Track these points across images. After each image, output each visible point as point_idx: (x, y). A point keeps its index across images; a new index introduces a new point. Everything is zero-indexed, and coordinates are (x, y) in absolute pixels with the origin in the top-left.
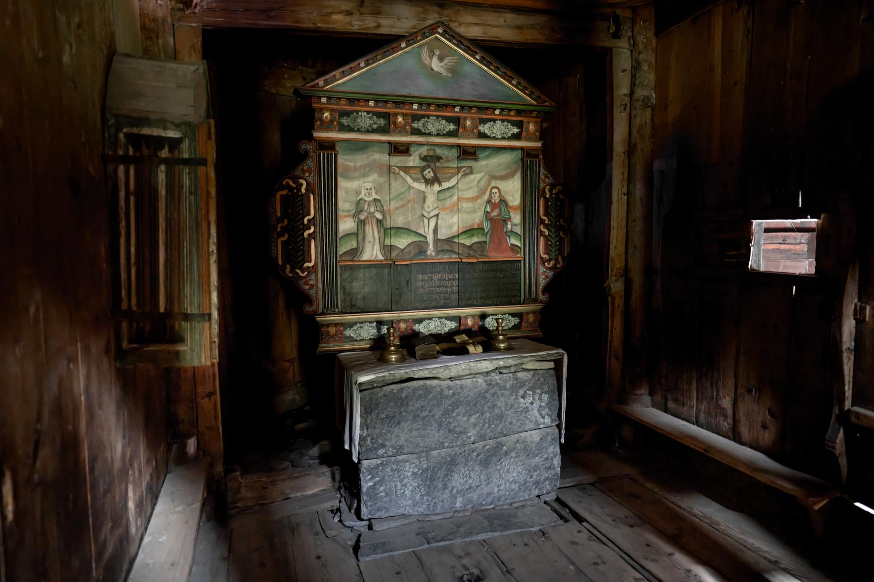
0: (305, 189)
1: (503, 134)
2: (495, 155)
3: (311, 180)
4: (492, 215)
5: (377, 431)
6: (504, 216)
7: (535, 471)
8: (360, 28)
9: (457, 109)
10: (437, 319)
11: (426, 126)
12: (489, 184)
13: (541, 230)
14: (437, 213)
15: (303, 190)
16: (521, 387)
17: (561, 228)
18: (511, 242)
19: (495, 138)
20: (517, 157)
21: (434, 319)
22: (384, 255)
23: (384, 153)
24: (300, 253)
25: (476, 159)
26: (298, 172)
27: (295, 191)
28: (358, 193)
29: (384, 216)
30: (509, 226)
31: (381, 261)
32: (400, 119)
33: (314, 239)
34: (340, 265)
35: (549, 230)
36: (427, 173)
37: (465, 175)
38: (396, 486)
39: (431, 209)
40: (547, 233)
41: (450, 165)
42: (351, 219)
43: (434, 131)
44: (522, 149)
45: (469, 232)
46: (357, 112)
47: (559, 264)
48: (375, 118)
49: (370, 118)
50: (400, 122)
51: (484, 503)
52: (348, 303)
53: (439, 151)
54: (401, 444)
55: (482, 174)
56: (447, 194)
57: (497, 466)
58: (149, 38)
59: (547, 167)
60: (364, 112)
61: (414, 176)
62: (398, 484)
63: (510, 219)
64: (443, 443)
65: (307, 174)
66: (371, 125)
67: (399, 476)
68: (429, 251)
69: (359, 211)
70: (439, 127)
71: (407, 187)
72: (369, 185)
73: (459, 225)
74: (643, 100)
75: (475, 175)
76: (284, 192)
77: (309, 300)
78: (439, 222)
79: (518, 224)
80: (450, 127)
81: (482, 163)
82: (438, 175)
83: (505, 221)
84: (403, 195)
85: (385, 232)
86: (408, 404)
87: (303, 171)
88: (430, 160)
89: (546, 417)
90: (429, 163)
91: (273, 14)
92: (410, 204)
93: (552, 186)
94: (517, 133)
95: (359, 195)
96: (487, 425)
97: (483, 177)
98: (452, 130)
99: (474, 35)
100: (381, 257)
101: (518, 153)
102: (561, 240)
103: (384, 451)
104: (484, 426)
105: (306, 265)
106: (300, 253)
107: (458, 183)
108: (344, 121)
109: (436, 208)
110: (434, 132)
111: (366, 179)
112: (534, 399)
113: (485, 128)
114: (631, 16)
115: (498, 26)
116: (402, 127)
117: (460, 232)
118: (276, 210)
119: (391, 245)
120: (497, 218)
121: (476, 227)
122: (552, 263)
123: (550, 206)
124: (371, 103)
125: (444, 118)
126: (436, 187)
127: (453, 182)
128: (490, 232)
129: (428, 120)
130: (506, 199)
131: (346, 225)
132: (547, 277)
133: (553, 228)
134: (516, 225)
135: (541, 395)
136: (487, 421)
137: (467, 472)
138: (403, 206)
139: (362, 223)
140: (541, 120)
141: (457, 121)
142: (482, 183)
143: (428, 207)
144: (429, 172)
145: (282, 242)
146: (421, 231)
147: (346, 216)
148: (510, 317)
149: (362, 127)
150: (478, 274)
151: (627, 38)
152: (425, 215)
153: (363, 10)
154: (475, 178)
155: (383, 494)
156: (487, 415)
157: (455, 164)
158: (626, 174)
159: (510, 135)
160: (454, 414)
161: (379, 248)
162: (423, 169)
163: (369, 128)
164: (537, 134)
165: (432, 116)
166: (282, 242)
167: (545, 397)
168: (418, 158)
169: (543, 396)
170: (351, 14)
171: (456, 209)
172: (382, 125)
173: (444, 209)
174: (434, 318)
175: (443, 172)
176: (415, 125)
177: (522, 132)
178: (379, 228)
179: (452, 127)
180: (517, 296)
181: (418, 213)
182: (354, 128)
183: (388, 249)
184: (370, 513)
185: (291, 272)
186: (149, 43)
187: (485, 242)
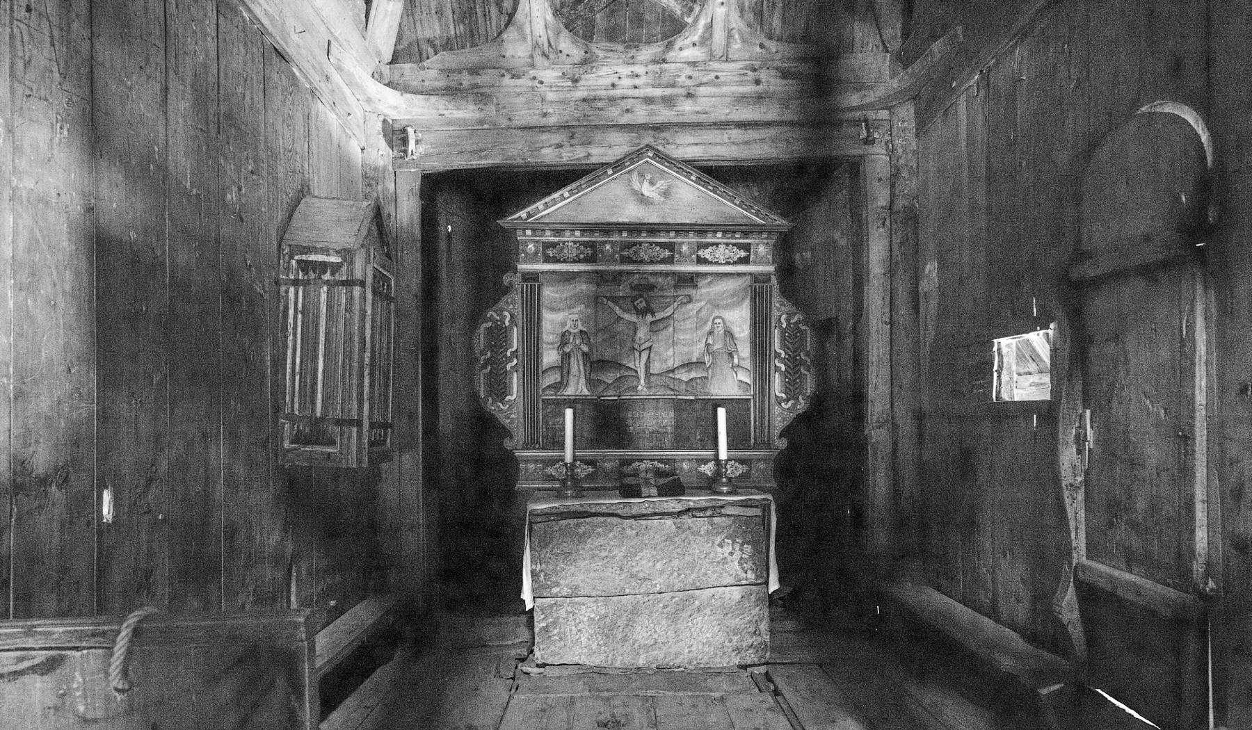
4: (715, 348)
5: (551, 567)
7: (735, 634)
14: (650, 344)
15: (507, 323)
16: (719, 533)
19: (717, 263)
24: (503, 386)
25: (695, 286)
26: (502, 304)
29: (591, 349)
30: (736, 361)
37: (683, 304)
38: (571, 630)
39: (643, 341)
42: (555, 352)
51: (672, 664)
53: (652, 280)
54: (576, 583)
57: (688, 622)
58: (369, 185)
62: (573, 628)
64: (623, 589)
65: (511, 307)
66: (577, 256)
67: (575, 620)
68: (640, 387)
72: (575, 317)
78: (652, 355)
81: (704, 291)
86: (586, 542)
87: (507, 303)
89: (749, 572)
91: (484, 153)
93: (790, 315)
96: (676, 574)
100: (587, 393)
103: (558, 590)
104: (672, 574)
105: (508, 398)
106: (503, 386)
112: (734, 549)
113: (706, 254)
117: (675, 366)
121: (694, 360)
126: (649, 318)
127: (669, 312)
132: (784, 419)
134: (743, 359)
135: (742, 545)
136: (676, 569)
137: (652, 625)
139: (566, 357)
144: (641, 302)
146: (631, 365)
148: (737, 464)
151: (883, 143)
153: (574, 142)
155: (556, 638)
156: (676, 563)
157: (672, 292)
158: (888, 299)
159: (735, 259)
160: (638, 558)
162: (634, 299)
167: (748, 548)
169: (745, 546)
170: (561, 146)
184: (542, 658)
186: (369, 189)
187: (706, 378)
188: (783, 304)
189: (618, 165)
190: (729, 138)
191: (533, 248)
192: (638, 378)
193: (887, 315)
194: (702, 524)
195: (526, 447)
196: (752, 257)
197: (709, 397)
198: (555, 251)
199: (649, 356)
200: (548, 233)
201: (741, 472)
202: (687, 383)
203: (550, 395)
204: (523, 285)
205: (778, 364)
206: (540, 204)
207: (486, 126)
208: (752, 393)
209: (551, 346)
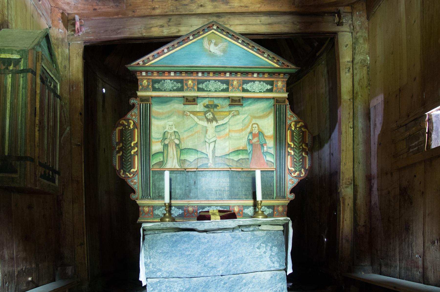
0: (133, 126)
1: (260, 89)
2: (254, 103)
3: (136, 121)
6: (262, 142)
8: (168, 33)
9: (228, 75)
10: (214, 207)
11: (208, 86)
12: (251, 121)
13: (288, 151)
14: (215, 140)
15: (132, 127)
17: (303, 150)
18: (267, 159)
19: (254, 92)
20: (271, 103)
21: (212, 207)
22: (180, 165)
23: (180, 103)
26: (129, 116)
27: (127, 127)
28: (164, 128)
30: (265, 149)
31: (178, 169)
32: (190, 82)
33: (137, 155)
34: (152, 171)
35: (294, 151)
36: (209, 115)
37: (234, 116)
39: (211, 137)
40: (293, 153)
41: (224, 110)
43: (213, 89)
44: (274, 98)
45: (237, 151)
46: (164, 80)
47: (302, 174)
48: (175, 83)
49: (172, 83)
50: (190, 84)
52: (157, 194)
53: (216, 102)
55: (246, 116)
56: (222, 128)
59: (292, 109)
60: (169, 80)
61: (200, 117)
63: (266, 144)
65: (134, 117)
66: (172, 87)
69: (164, 139)
70: (217, 87)
71: (195, 123)
72: (171, 123)
73: (230, 148)
74: (361, 62)
75: (241, 116)
76: (121, 128)
77: (133, 191)
78: (216, 145)
79: (272, 147)
80: (223, 86)
82: (216, 116)
83: (262, 146)
84: (192, 128)
85: (180, 152)
87: (132, 115)
88: (210, 107)
90: (209, 109)
92: (196, 134)
93: (296, 123)
94: (270, 89)
95: (165, 129)
97: (247, 117)
98: (224, 88)
99: (240, 31)
100: (178, 167)
101: (272, 102)
102: (303, 158)
105: (132, 170)
106: (129, 163)
107: (229, 121)
108: (156, 85)
109: (214, 137)
110: (213, 90)
111: (169, 120)
113: (247, 86)
114: (350, 11)
115: (255, 25)
116: (192, 87)
117: (230, 152)
118: (116, 138)
119: (185, 159)
120: (257, 143)
121: (241, 148)
122: (297, 173)
123: (295, 135)
124: (172, 74)
125: (219, 81)
126: (214, 124)
128: (251, 152)
129: (209, 83)
130: (263, 131)
131: (156, 147)
133: (297, 150)
134: (270, 148)
138: (192, 135)
140: (287, 79)
141: (227, 82)
142: (246, 121)
143: (209, 136)
144: (210, 115)
145: (119, 156)
146: (204, 151)
147: (157, 142)
149: (167, 89)
150: (243, 179)
152: (206, 141)
154: (240, 117)
157: (228, 109)
158: (351, 114)
159: (265, 90)
161: (177, 161)
162: (205, 113)
163: (171, 89)
164: (284, 88)
165: (211, 80)
166: (119, 156)
168: (202, 106)
171: (228, 137)
172: (180, 87)
173: (220, 137)
174: (212, 206)
175: (219, 115)
176: (200, 86)
177: (273, 87)
178: (177, 149)
179: (225, 86)
180: (271, 195)
181: (203, 140)
182: (162, 90)
183: (182, 162)
185: (123, 174)
187: (248, 159)
188: (292, 116)
189: (196, 34)
190: (260, 21)
191: (146, 83)
192: (208, 159)
193: (351, 123)
194: (247, 235)
195: (143, 198)
196: (274, 89)
197: (250, 170)
198: (159, 85)
199: (215, 147)
200: (155, 74)
201: (268, 213)
202: (237, 161)
203: (156, 168)
204: (140, 104)
205: (290, 151)
206: (150, 56)
207: (120, 16)
208: (275, 167)
209: (157, 140)
